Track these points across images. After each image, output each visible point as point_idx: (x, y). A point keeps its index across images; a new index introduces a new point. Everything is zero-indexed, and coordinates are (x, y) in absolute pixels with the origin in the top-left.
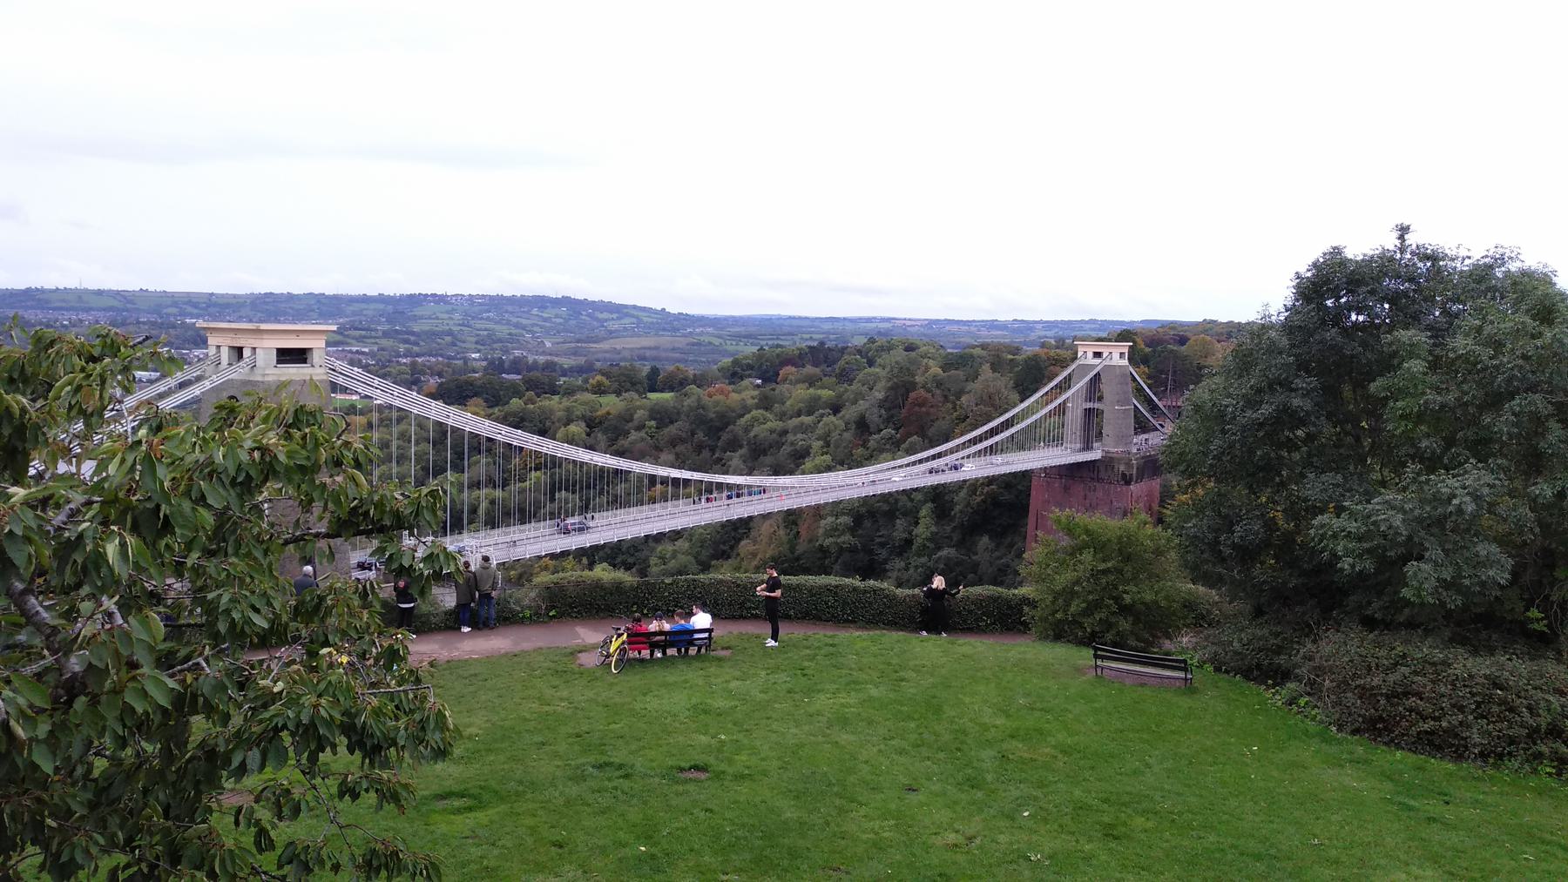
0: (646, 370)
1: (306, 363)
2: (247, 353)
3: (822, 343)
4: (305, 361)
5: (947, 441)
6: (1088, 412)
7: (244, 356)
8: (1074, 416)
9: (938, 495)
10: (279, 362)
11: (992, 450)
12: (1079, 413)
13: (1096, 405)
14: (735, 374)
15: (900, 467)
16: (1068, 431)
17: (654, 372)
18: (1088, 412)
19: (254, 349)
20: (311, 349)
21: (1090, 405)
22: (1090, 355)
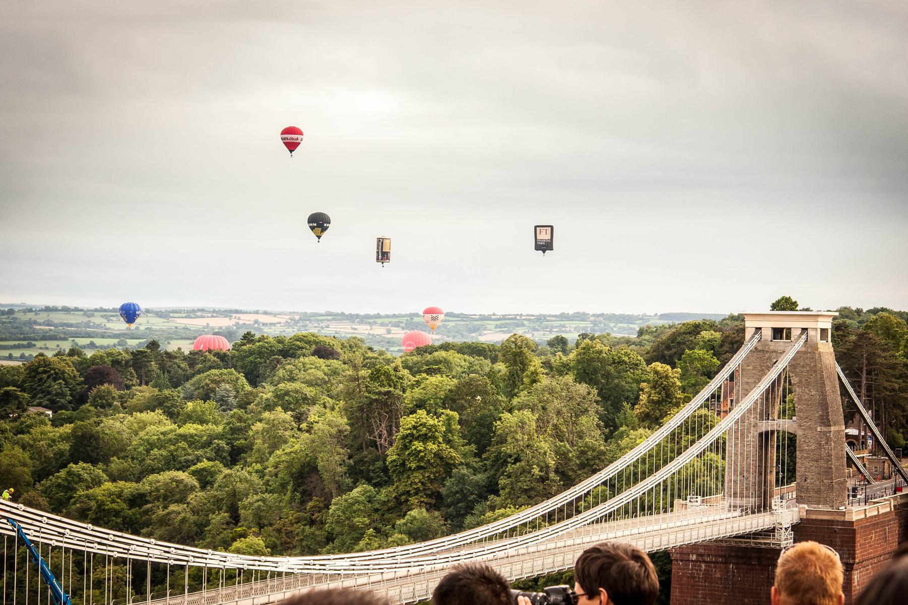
6: (765, 438)
12: (752, 438)
13: (786, 425)
18: (765, 438)
22: (767, 334)
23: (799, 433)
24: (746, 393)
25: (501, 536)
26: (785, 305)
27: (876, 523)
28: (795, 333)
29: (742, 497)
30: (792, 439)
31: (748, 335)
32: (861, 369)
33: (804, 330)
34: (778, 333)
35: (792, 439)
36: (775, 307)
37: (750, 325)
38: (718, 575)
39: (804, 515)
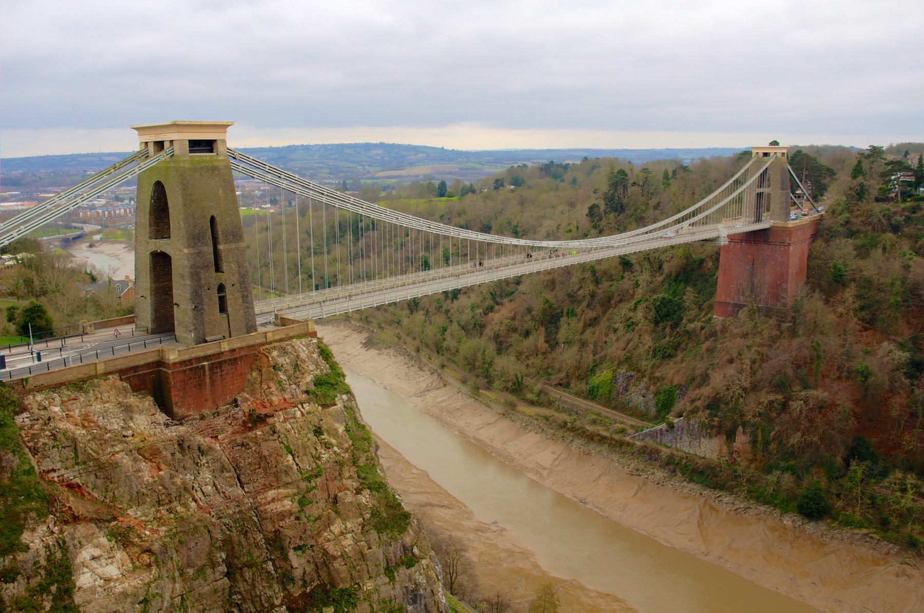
0: (437, 183)
1: (212, 152)
2: (167, 145)
3: (552, 162)
4: (211, 151)
5: (655, 222)
6: (760, 195)
7: (165, 148)
8: (749, 202)
9: (652, 260)
10: (191, 151)
11: (704, 222)
13: (765, 190)
14: (499, 184)
15: (638, 235)
16: (744, 210)
17: (443, 185)
19: (172, 141)
20: (216, 140)
21: (759, 190)
22: (761, 155)
23: (772, 193)
24: (751, 177)
25: (642, 234)
26: (775, 143)
27: (801, 228)
28: (772, 155)
29: (749, 217)
30: (769, 195)
31: (753, 156)
32: (803, 168)
33: (776, 153)
34: (766, 155)
35: (769, 195)
36: (772, 144)
37: (754, 151)
38: (738, 247)
39: (772, 224)
